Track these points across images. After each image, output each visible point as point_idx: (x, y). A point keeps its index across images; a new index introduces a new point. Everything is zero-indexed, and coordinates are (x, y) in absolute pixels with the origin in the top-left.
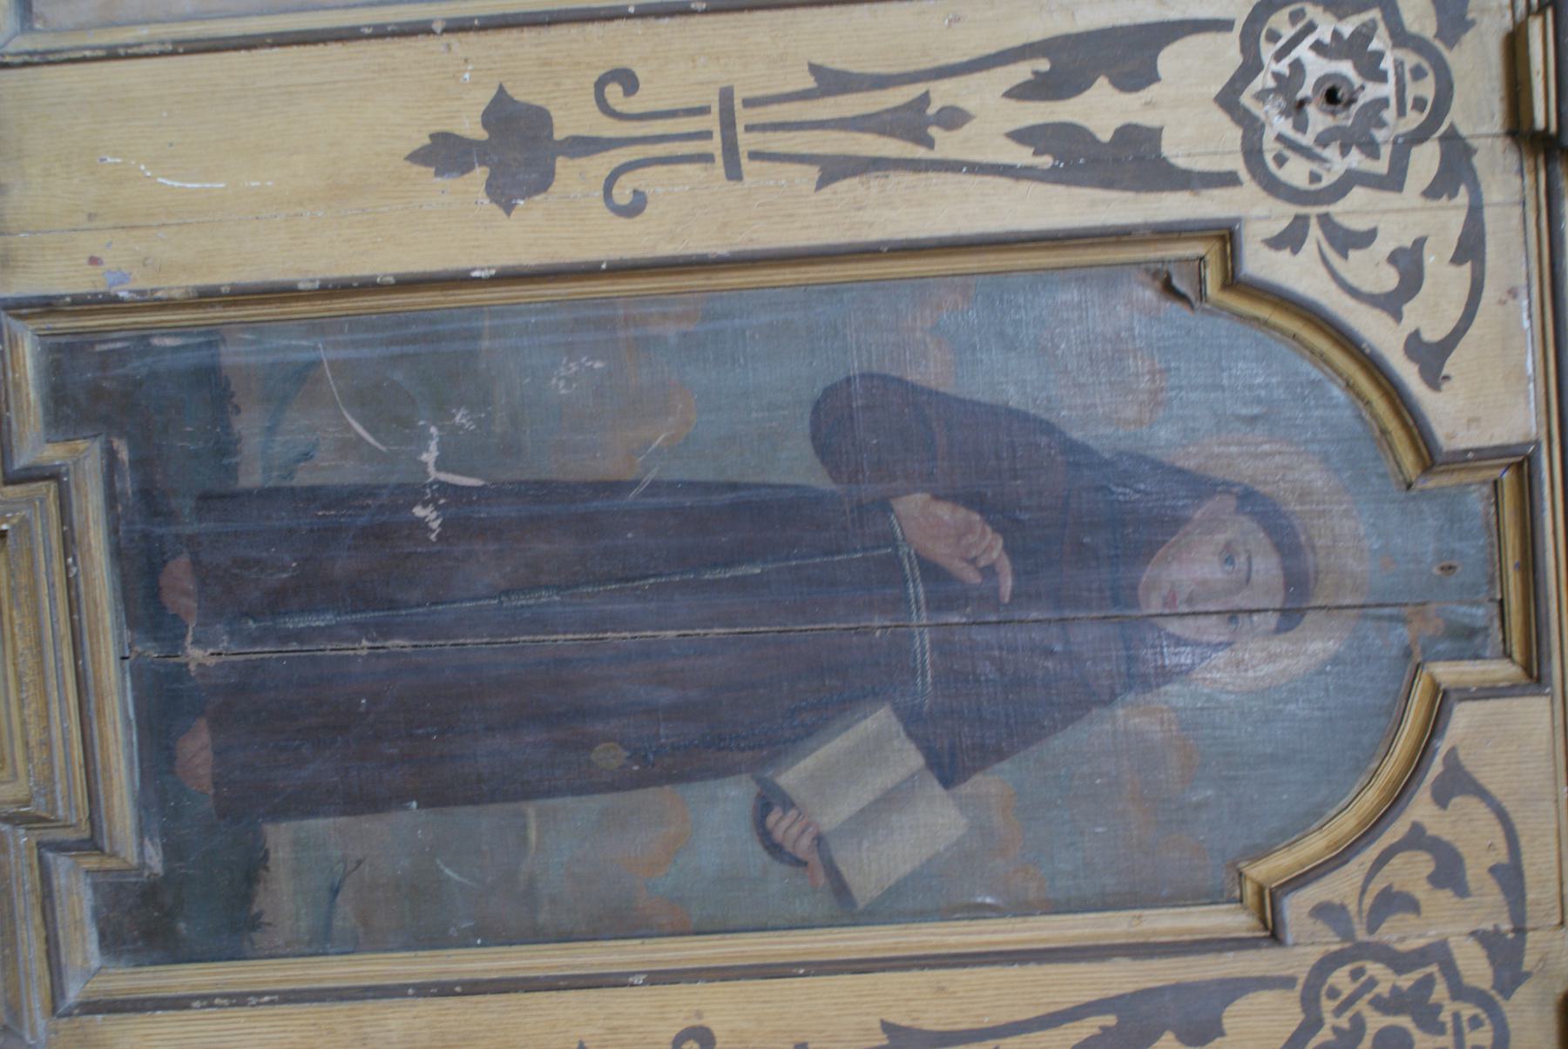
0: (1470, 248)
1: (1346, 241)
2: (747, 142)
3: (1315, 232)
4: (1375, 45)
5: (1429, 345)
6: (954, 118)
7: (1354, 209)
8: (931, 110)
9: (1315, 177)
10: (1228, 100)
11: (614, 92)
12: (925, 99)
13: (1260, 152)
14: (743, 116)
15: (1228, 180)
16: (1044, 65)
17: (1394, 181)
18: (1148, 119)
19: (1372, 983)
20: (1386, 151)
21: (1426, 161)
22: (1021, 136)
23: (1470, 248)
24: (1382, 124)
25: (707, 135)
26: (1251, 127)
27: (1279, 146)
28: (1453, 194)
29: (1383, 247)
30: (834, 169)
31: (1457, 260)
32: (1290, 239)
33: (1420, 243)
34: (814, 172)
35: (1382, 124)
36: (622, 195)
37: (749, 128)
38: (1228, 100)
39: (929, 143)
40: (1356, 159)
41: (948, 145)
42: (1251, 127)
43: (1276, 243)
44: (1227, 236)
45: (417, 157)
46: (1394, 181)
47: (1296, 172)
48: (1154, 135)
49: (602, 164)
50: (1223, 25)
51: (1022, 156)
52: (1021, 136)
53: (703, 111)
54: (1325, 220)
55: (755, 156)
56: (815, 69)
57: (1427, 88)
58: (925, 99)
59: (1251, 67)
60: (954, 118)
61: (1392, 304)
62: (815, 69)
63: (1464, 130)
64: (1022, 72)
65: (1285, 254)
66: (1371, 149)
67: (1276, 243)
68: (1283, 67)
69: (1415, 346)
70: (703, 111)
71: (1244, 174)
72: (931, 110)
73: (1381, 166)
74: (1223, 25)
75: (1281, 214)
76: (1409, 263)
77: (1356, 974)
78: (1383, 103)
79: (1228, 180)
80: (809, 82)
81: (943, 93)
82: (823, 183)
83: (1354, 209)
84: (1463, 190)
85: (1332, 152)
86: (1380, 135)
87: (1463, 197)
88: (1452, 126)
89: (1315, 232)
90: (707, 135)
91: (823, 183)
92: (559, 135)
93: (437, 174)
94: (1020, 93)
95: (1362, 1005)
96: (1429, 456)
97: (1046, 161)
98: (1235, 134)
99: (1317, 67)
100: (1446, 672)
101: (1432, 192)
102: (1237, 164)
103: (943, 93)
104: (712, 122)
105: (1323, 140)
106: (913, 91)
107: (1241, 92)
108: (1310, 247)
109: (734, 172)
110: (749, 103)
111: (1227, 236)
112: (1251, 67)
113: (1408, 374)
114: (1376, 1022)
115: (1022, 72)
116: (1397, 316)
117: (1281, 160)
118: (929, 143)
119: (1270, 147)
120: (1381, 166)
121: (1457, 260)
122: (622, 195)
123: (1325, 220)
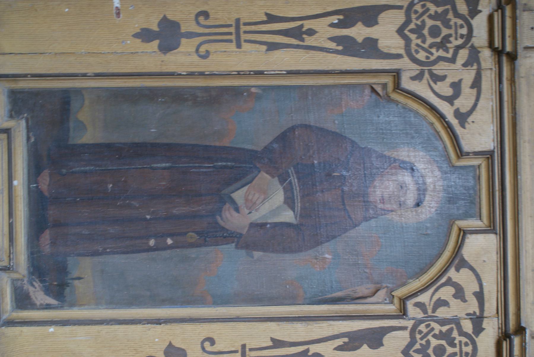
0: (477, 84)
1: (437, 78)
2: (244, 37)
3: (427, 75)
4: (448, 17)
5: (462, 114)
6: (311, 32)
7: (440, 69)
8: (304, 29)
9: (428, 58)
10: (400, 31)
11: (201, 19)
12: (302, 26)
13: (410, 50)
14: (243, 28)
15: (399, 56)
16: (341, 17)
17: (453, 60)
18: (374, 36)
19: (433, 329)
20: (451, 51)
21: (463, 55)
22: (332, 39)
23: (477, 84)
24: (450, 42)
25: (230, 34)
26: (408, 41)
27: (417, 48)
28: (472, 66)
29: (449, 80)
30: (272, 47)
31: (472, 87)
32: (419, 77)
33: (460, 81)
34: (264, 48)
35: (450, 42)
36: (203, 49)
37: (245, 32)
38: (400, 31)
39: (303, 40)
40: (441, 53)
41: (309, 41)
42: (408, 41)
43: (413, 78)
44: (397, 74)
45: (136, 36)
46: (453, 60)
47: (421, 56)
48: (376, 41)
49: (197, 40)
50: (400, 7)
51: (332, 45)
52: (332, 39)
53: (230, 26)
54: (430, 72)
55: (246, 41)
56: (267, 14)
57: (464, 31)
58: (302, 26)
59: (408, 21)
60: (311, 32)
61: (450, 100)
62: (267, 14)
63: (476, 45)
64: (335, 19)
65: (416, 82)
66: (447, 50)
67: (413, 78)
68: (419, 23)
69: (457, 114)
70: (230, 26)
71: (405, 55)
72: (304, 29)
73: (449, 55)
74: (400, 7)
75: (415, 69)
76: (456, 86)
77: (428, 326)
78: (450, 35)
79: (399, 56)
80: (265, 18)
81: (308, 25)
82: (268, 50)
83: (440, 69)
84: (475, 64)
85: (433, 50)
86: (449, 45)
87: (475, 67)
88: (472, 44)
89: (427, 75)
90: (230, 34)
91: (268, 50)
92: (183, 29)
93: (143, 41)
94: (332, 25)
95: (430, 337)
96: (461, 153)
97: (340, 48)
98: (401, 42)
99: (430, 23)
100: (464, 224)
101: (465, 65)
102: (402, 52)
103: (308, 25)
104: (232, 30)
105: (431, 46)
106: (299, 23)
107: (404, 30)
108: (424, 81)
109: (239, 46)
110: (245, 24)
111: (397, 74)
112: (408, 21)
113: (454, 122)
114: (434, 342)
115: (335, 19)
116: (452, 104)
117: (417, 52)
118: (303, 40)
119: (413, 46)
120: (449, 55)
121: (472, 87)
122: (203, 49)
123: (430, 72)
